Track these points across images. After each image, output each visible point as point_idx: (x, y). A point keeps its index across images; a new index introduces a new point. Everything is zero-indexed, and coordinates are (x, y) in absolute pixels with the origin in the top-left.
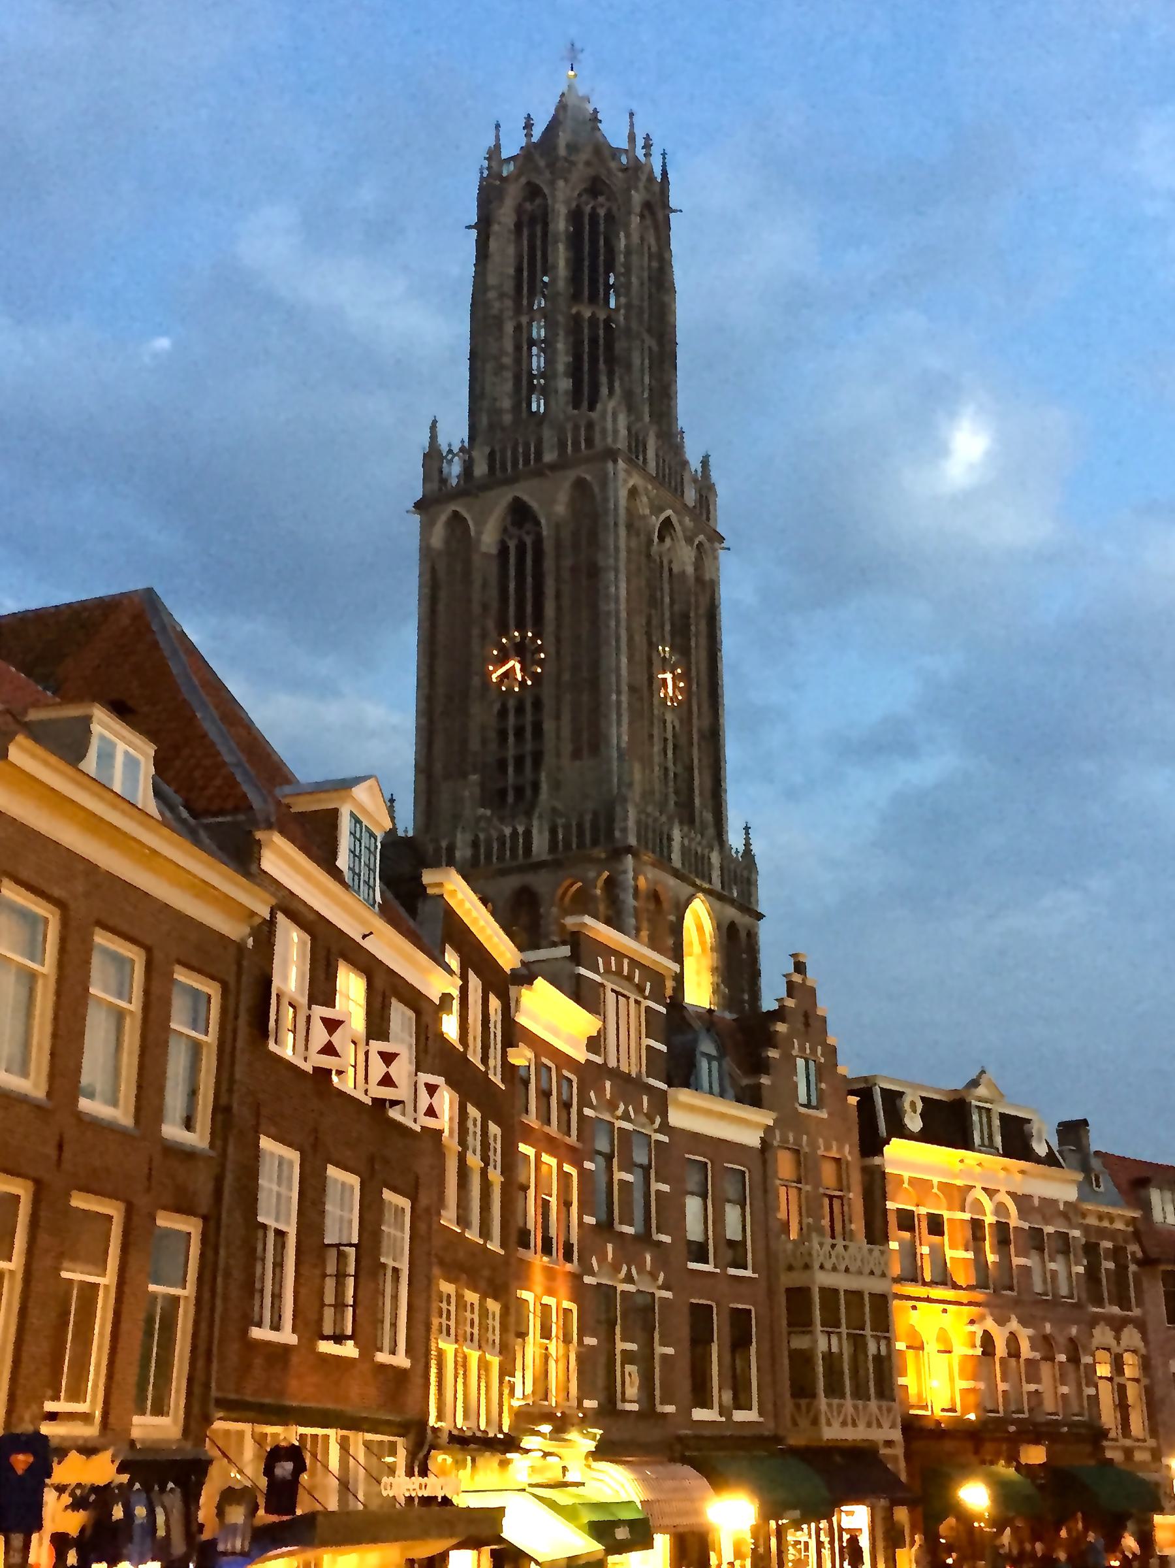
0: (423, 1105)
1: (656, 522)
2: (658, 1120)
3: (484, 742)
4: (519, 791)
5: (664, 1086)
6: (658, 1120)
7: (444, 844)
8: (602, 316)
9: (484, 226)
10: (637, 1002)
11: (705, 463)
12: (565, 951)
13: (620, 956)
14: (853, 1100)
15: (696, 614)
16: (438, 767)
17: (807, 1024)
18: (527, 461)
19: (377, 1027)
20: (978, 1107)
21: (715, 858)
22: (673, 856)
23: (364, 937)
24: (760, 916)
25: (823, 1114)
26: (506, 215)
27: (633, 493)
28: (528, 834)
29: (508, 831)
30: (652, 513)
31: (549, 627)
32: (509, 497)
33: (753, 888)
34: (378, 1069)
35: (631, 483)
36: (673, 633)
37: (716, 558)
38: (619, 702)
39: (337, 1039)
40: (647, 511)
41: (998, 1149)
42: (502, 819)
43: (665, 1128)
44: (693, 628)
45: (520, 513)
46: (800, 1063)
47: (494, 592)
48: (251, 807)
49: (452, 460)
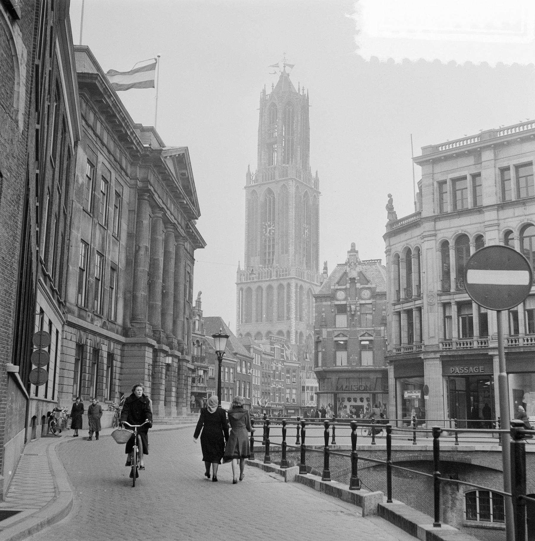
1: (303, 193)
4: (269, 260)
11: (317, 172)
21: (316, 276)
27: (297, 187)
29: (266, 271)
37: (318, 198)
42: (265, 268)
43: (284, 365)
45: (270, 191)
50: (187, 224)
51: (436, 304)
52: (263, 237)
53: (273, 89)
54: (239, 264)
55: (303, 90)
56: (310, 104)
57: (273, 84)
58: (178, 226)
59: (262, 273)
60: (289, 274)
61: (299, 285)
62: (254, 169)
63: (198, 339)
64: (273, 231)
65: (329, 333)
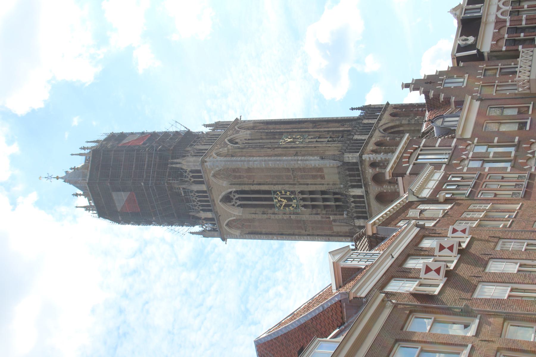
0: (462, 235)
1: (230, 145)
3: (317, 214)
4: (337, 200)
5: (455, 140)
10: (421, 150)
11: (207, 126)
12: (400, 179)
13: (402, 157)
14: (461, 64)
15: (266, 129)
16: (329, 232)
17: (430, 83)
18: (206, 197)
19: (428, 253)
20: (464, 14)
22: (363, 138)
23: (393, 257)
24: (388, 104)
25: (467, 76)
27: (218, 154)
28: (354, 197)
29: (353, 205)
33: (376, 107)
34: (446, 252)
35: (216, 156)
36: (274, 138)
37: (244, 121)
38: (301, 160)
39: (434, 268)
40: (226, 149)
41: (482, 6)
42: (348, 207)
43: (472, 139)
44: (272, 131)
45: (227, 199)
46: (446, 85)
47: (258, 210)
48: (340, 301)
52: (299, 211)
53: (80, 195)
55: (84, 148)
57: (73, 195)
60: (356, 164)
61: (375, 147)
64: (288, 193)
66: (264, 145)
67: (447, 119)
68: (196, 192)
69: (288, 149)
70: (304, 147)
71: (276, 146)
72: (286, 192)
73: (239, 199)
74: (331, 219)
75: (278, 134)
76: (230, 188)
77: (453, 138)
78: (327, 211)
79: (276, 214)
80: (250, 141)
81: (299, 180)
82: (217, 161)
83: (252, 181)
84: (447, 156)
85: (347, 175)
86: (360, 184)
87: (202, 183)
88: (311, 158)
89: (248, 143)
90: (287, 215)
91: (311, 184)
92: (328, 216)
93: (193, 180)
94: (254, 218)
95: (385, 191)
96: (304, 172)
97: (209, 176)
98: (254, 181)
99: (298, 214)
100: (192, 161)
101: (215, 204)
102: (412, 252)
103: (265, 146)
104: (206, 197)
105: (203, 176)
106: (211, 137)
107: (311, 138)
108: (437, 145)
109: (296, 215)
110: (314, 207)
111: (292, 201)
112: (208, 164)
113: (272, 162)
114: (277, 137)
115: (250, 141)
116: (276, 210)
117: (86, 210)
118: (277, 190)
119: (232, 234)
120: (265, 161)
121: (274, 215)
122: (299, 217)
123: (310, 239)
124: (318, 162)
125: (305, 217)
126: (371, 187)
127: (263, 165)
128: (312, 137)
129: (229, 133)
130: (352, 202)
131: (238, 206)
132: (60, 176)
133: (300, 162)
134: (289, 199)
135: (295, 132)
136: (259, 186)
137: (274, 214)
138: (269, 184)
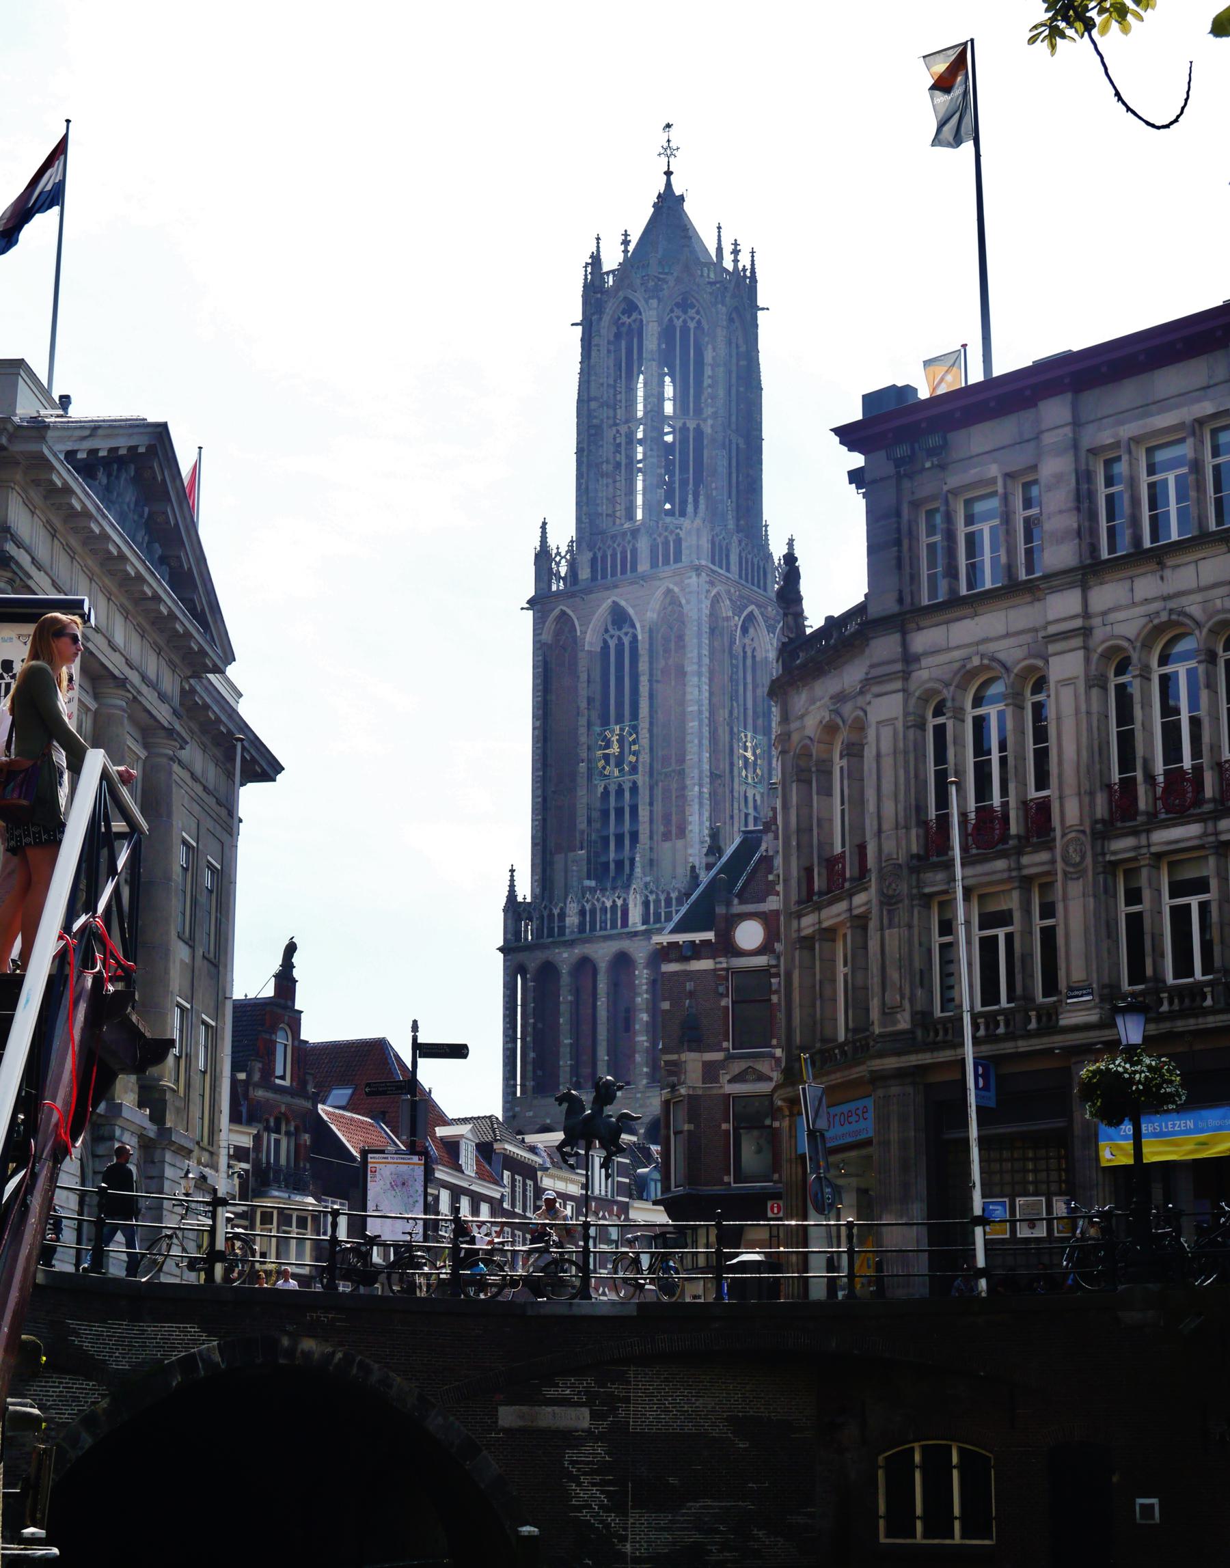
1: (738, 621)
2: (623, 1217)
3: (589, 822)
4: (619, 864)
5: (627, 1200)
6: (623, 1217)
7: (556, 912)
8: (691, 425)
9: (589, 325)
11: (791, 543)
26: (605, 326)
27: (716, 601)
29: (609, 904)
30: (734, 614)
31: (644, 725)
32: (609, 601)
35: (714, 592)
40: (730, 614)
42: (603, 890)
45: (619, 617)
47: (597, 687)
49: (560, 562)
50: (193, 691)
51: (906, 902)
53: (626, 251)
54: (512, 880)
55: (736, 252)
56: (760, 303)
57: (626, 235)
58: (145, 689)
59: (593, 911)
62: (563, 535)
63: (283, 1109)
64: (633, 759)
65: (710, 1072)
66: (737, 702)
67: (659, 1185)
68: (634, 546)
69: (727, 757)
70: (732, 791)
71: (735, 730)
72: (635, 753)
73: (620, 644)
74: (580, 852)
75: (766, 724)
76: (643, 627)
77: (631, 1197)
78: (596, 842)
79: (589, 729)
80: (749, 662)
81: (660, 784)
82: (700, 602)
83: (659, 678)
84: (603, 1193)
85: (668, 894)
86: (652, 920)
87: (654, 564)
88: (706, 814)
89: (745, 657)
90: (585, 755)
91: (651, 812)
92: (585, 844)
93: (659, 540)
94: (578, 677)
95: (637, 972)
96: (677, 797)
97: (666, 581)
98: (657, 681)
99: (590, 778)
100: (700, 543)
101: (607, 589)
102: (475, 1200)
103: (735, 704)
104: (624, 572)
105: (666, 568)
106: (759, 567)
107: (755, 801)
108: (620, 1179)
109: (586, 775)
110: (605, 813)
111: (616, 767)
112: (693, 580)
113: (697, 727)
114: (760, 721)
115: (749, 662)
116: (598, 729)
117: (592, 257)
118: (640, 736)
119: (544, 623)
120: (700, 712)
121: (585, 724)
122: (582, 781)
123: (537, 803)
124: (697, 831)
125: (582, 792)
126: (644, 943)
127: (692, 708)
128: (759, 802)
129: (770, 609)
130: (614, 901)
131: (605, 642)
132: (672, 177)
133: (697, 790)
134: (620, 762)
135: (770, 764)
136: (647, 694)
137: (589, 725)
138: (651, 717)
